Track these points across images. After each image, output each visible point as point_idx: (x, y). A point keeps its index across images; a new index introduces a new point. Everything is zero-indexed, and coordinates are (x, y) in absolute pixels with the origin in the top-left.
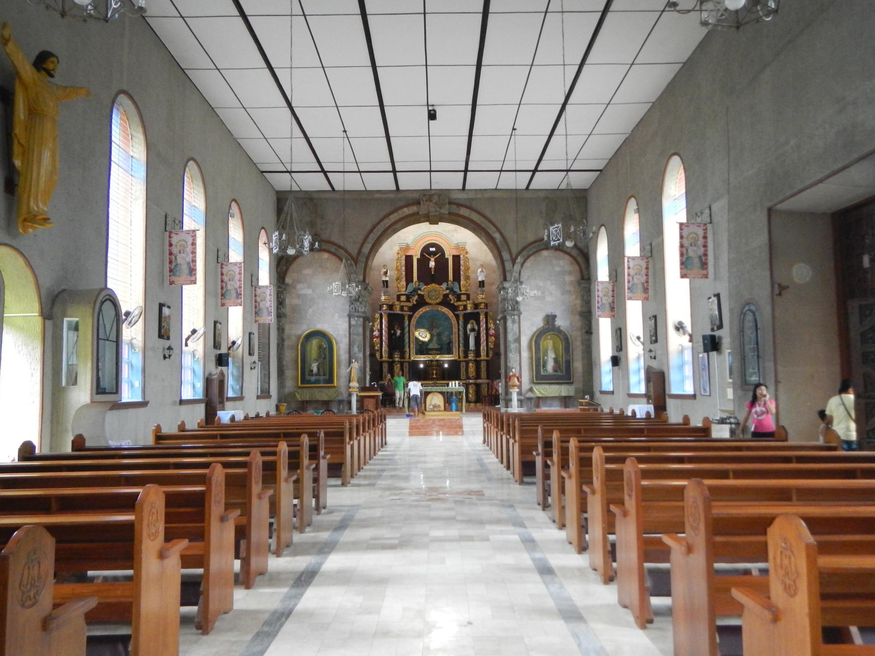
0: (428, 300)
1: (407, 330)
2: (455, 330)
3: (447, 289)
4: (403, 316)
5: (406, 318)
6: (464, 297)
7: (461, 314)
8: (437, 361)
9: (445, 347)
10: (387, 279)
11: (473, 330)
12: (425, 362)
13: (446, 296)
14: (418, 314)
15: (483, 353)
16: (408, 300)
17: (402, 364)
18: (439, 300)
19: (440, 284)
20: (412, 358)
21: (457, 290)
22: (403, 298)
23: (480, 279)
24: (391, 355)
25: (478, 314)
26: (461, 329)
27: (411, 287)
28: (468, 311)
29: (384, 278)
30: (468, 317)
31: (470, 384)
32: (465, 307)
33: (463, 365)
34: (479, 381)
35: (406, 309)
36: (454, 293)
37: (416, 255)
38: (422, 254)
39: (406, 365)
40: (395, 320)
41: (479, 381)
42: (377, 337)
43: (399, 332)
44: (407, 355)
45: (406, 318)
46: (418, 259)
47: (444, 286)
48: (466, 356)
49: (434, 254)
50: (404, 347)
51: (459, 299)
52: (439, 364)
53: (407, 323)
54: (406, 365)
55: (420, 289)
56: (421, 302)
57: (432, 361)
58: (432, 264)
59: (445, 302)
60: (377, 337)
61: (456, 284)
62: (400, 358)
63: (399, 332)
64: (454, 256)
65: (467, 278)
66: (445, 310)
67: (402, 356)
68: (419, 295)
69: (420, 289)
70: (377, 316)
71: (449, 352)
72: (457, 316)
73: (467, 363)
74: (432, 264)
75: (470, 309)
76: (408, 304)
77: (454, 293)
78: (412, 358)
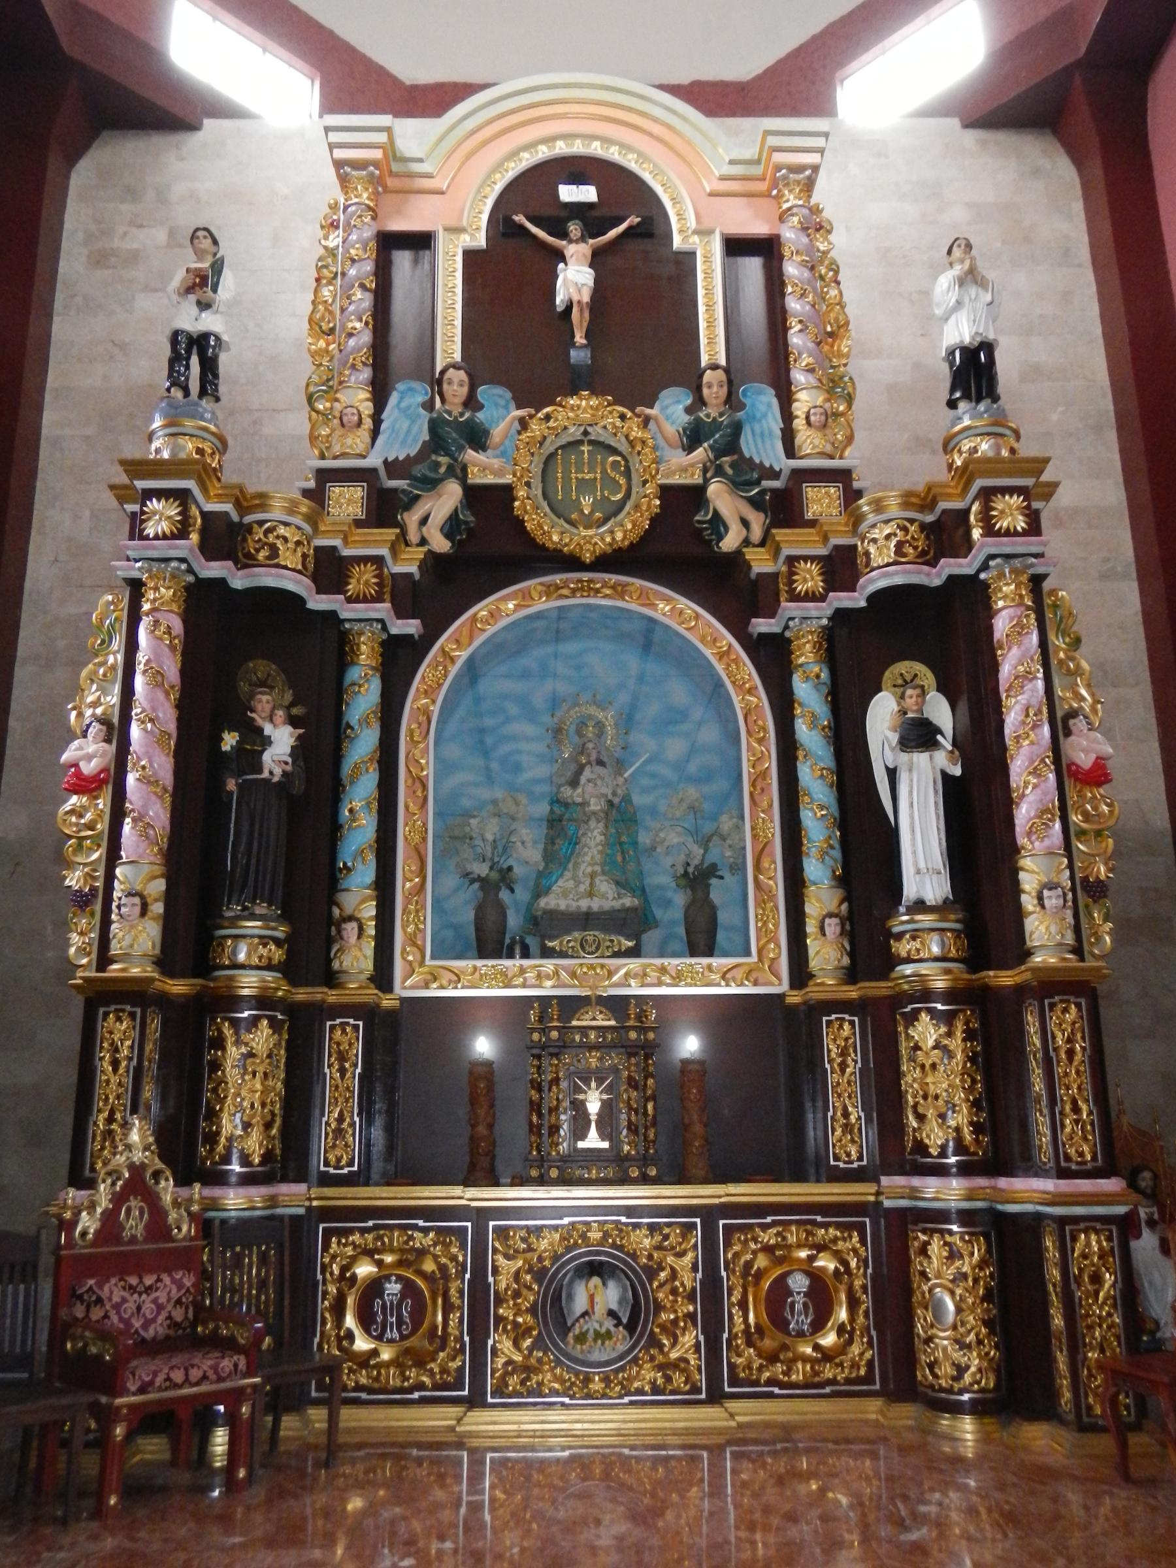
0: (555, 534)
1: (363, 745)
2: (758, 753)
3: (693, 437)
4: (335, 638)
5: (366, 654)
6: (821, 501)
7: (803, 620)
8: (616, 1005)
9: (673, 907)
10: (209, 322)
11: (918, 735)
12: (512, 1015)
13: (682, 501)
14: (457, 645)
15: (1044, 931)
16: (384, 509)
17: (302, 1032)
18: (623, 530)
19: (636, 394)
20: (408, 985)
21: (772, 455)
22: (348, 501)
23: (961, 331)
24: (191, 938)
25: (971, 596)
26: (811, 737)
27: (405, 431)
28: (874, 582)
29: (191, 320)
30: (863, 647)
31: (934, 1218)
32: (842, 567)
33: (840, 1038)
34: (1027, 1192)
35: (362, 579)
36: (745, 474)
37: (460, 218)
38: (503, 225)
39: (346, 1041)
40: (241, 638)
41: (1027, 1192)
42: (85, 785)
43: (281, 742)
44: (356, 957)
45: (366, 654)
46: (471, 257)
47: (672, 409)
48: (870, 949)
49: (592, 219)
50: (331, 879)
51: (784, 508)
52: (636, 1031)
53: (364, 697)
54: (346, 1041)
55: (477, 438)
56: (493, 548)
57: (571, 1005)
58: (575, 279)
59: (674, 546)
60: (85, 785)
61: (762, 401)
62: (291, 970)
63: (281, 742)
64: (736, 247)
65: (836, 386)
66: (674, 610)
67: (309, 952)
68: (474, 495)
69: (477, 438)
70: (108, 605)
71: (702, 939)
72: (773, 657)
73: (884, 1022)
74: (575, 279)
75: (886, 568)
76: (377, 544)
77: (745, 474)
78: (408, 985)
